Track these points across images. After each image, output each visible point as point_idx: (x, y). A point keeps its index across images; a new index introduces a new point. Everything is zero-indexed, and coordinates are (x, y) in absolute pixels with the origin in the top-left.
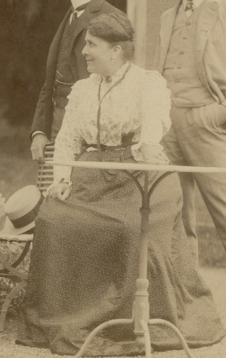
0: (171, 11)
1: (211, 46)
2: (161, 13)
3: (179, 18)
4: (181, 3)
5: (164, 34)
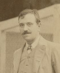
0: (20, 50)
1: (41, 70)
2: (14, 51)
3: (24, 54)
4: (25, 46)
5: (16, 63)
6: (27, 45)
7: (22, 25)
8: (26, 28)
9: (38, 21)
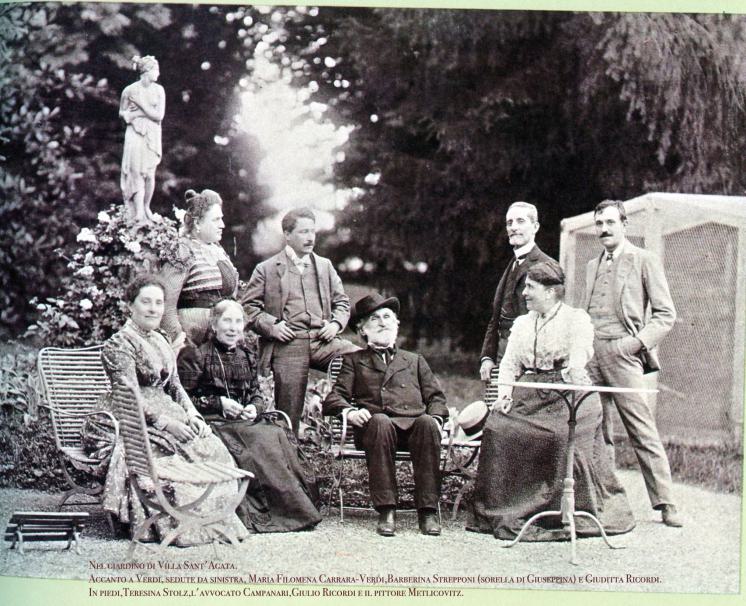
0: (596, 260)
1: (627, 290)
4: (603, 254)
5: (590, 279)
6: (607, 253)
7: (599, 223)
8: (605, 228)
9: (623, 218)
